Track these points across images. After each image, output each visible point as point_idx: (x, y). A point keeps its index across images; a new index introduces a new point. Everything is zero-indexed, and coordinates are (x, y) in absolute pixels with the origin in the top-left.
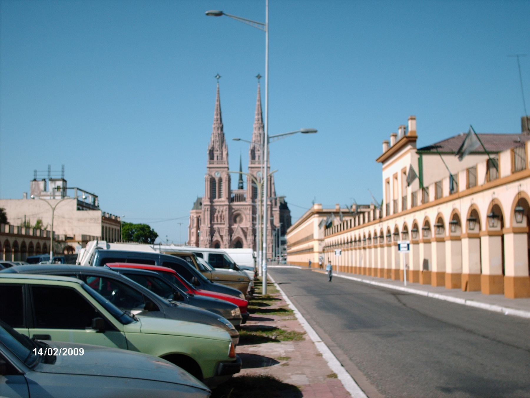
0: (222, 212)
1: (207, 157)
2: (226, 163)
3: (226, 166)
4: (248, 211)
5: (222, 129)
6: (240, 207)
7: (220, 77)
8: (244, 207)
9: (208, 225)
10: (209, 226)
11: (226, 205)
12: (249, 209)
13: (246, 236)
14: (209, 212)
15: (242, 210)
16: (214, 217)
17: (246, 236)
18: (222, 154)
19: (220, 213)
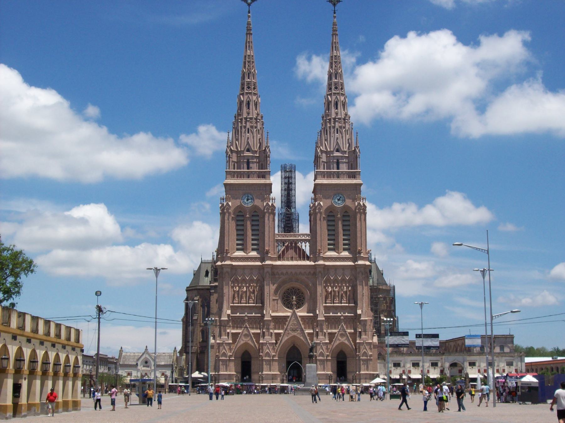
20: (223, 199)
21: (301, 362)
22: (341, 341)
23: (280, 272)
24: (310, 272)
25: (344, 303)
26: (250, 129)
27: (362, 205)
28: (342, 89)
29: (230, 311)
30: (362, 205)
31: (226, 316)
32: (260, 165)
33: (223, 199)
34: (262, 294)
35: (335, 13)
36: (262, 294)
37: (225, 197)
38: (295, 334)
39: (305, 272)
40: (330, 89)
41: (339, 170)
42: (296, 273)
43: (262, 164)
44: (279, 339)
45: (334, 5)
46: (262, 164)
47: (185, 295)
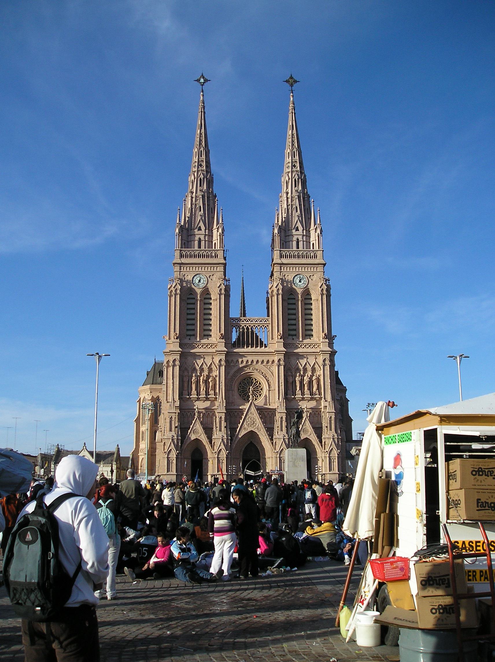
0: (210, 370)
1: (177, 242)
2: (220, 254)
4: (275, 369)
5: (210, 183)
7: (206, 81)
8: (265, 359)
9: (174, 401)
10: (178, 404)
11: (219, 352)
12: (276, 361)
13: (270, 432)
14: (177, 368)
16: (190, 383)
17: (270, 432)
18: (211, 236)
19: (206, 373)
21: (259, 460)
23: (235, 360)
25: (308, 394)
34: (215, 384)
36: (215, 384)
44: (235, 435)
45: (292, 85)
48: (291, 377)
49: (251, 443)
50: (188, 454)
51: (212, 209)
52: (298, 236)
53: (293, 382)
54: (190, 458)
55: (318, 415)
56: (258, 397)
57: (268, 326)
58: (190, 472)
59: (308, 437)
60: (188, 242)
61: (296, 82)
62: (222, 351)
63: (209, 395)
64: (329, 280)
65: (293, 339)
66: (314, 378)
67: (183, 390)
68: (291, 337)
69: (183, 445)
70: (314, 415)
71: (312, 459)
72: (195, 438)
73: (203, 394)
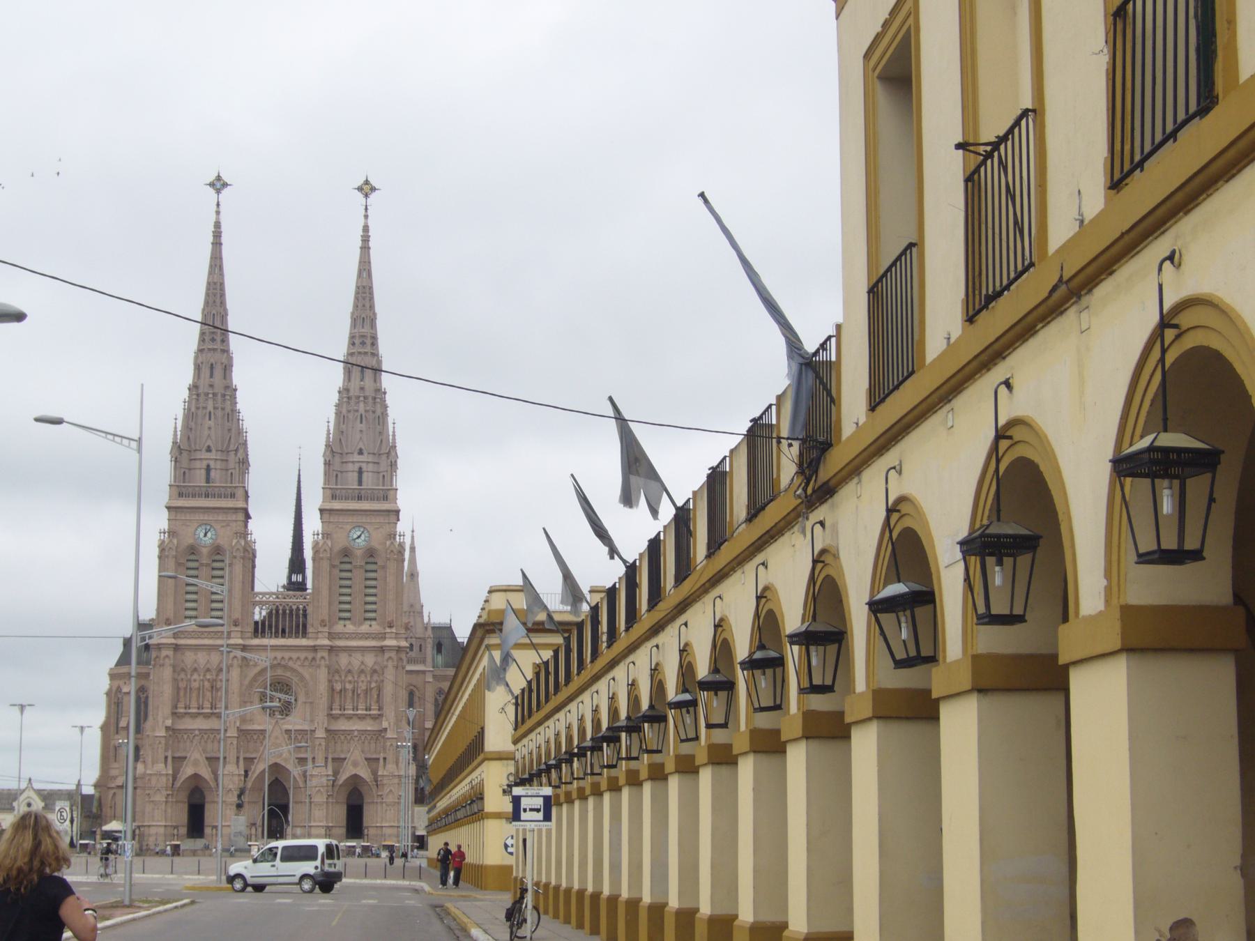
3: (241, 504)
6: (287, 655)
8: (303, 655)
15: (291, 664)
20: (165, 533)
22: (353, 773)
24: (306, 658)
25: (362, 709)
26: (212, 411)
27: (397, 546)
28: (373, 344)
29: (171, 721)
30: (397, 546)
31: (164, 730)
32: (229, 475)
33: (165, 533)
35: (366, 209)
37: (166, 530)
38: (278, 761)
39: (298, 658)
40: (353, 344)
41: (361, 485)
42: (283, 658)
43: (232, 474)
44: (251, 769)
45: (366, 196)
46: (232, 474)
47: (105, 683)
48: (339, 684)
49: (277, 779)
50: (184, 796)
51: (228, 414)
52: (361, 464)
53: (341, 691)
54: (186, 800)
55: (376, 740)
56: (289, 711)
57: (307, 605)
58: (186, 821)
59: (358, 773)
60: (190, 469)
61: (373, 189)
62: (236, 645)
63: (215, 708)
64: (404, 536)
65: (345, 626)
66: (373, 685)
67: (178, 701)
68: (342, 622)
69: (175, 783)
70: (371, 739)
71: (365, 808)
72: (193, 773)
73: (208, 708)
